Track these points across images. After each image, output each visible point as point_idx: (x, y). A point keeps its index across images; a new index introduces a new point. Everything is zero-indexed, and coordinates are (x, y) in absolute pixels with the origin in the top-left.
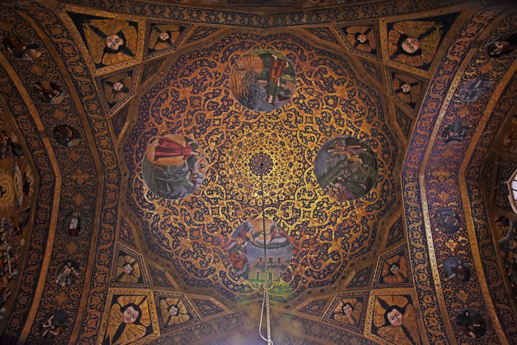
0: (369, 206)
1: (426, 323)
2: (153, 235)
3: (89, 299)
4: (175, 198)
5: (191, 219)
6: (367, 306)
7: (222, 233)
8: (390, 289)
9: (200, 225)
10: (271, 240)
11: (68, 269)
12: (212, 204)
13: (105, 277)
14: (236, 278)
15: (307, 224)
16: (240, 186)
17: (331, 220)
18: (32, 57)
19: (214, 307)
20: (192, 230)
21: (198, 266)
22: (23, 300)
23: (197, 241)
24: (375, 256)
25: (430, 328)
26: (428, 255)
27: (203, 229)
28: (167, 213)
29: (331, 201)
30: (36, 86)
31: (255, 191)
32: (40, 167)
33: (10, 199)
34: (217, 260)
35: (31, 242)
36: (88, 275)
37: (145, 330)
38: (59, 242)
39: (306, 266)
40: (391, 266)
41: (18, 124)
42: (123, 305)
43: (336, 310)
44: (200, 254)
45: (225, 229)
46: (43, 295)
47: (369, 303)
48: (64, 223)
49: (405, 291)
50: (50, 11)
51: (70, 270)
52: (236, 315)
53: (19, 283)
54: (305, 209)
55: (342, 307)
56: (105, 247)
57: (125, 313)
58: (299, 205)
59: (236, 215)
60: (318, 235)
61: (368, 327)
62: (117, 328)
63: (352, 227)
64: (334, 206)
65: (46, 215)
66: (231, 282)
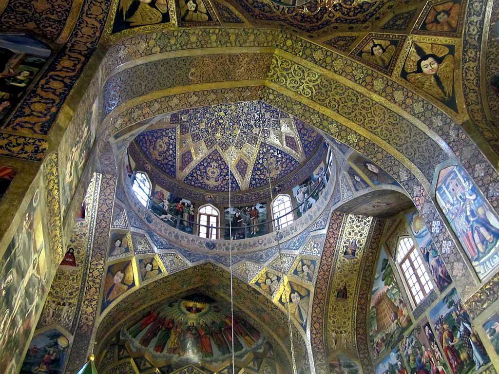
1: (464, 75)
8: (431, 37)
19: (233, 15)
25: (467, 80)
26: (485, 9)
37: (161, 16)
40: (439, 13)
47: (405, 46)
52: (255, 32)
55: (372, 48)
61: (397, 71)
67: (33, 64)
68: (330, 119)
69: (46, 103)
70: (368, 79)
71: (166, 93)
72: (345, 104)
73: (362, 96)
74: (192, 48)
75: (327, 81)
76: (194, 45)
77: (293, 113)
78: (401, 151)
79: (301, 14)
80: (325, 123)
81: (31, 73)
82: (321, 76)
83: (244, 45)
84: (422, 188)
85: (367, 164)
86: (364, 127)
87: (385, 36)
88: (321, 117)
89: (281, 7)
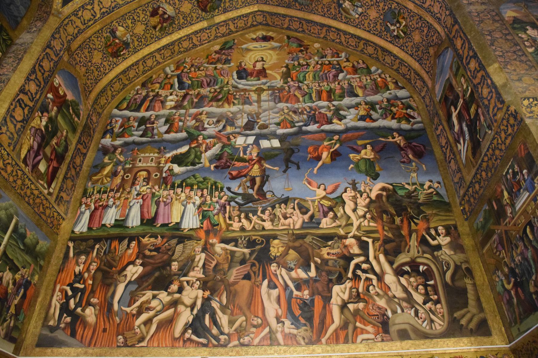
18: (126, 34)
22: (370, 50)
30: (157, 29)
32: (249, 25)
33: (270, 54)
35: (320, 38)
38: (320, 10)
41: (203, 44)
46: (368, 31)
48: (303, 4)
50: (63, 22)
51: (347, 2)
53: (355, 52)
65: (295, 21)
67: (458, 69)
69: (484, 84)
81: (463, 75)
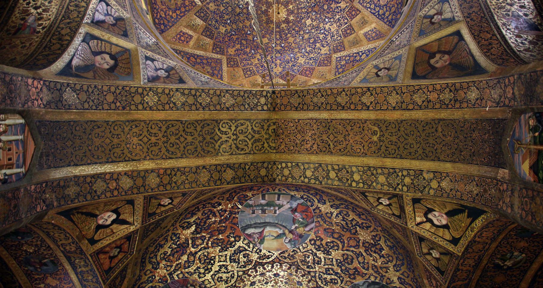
0: (151, 282)
1: (68, 235)
2: (402, 255)
3: (487, 247)
4: (374, 283)
5: (357, 258)
6: (143, 214)
7: (322, 240)
8: (118, 238)
9: (347, 250)
10: (263, 230)
11: (508, 264)
12: (332, 269)
13: (464, 262)
14: (305, 197)
15: (222, 249)
16: (300, 283)
17: (195, 257)
20: (357, 246)
21: (350, 213)
23: (351, 236)
24: (139, 251)
26: (78, 277)
27: (343, 246)
28: (384, 270)
29: (196, 276)
31: (283, 277)
34: (329, 215)
36: (485, 262)
37: (422, 202)
39: (221, 209)
40: (119, 253)
42: (446, 230)
43: (180, 198)
44: (349, 223)
45: (318, 243)
47: (140, 219)
49: (99, 245)
51: (506, 263)
52: (306, 180)
54: (224, 263)
55: (173, 201)
56: (460, 283)
57: (444, 222)
58: (232, 266)
59: (305, 255)
60: (209, 240)
61: (139, 201)
62: (456, 217)
63: (170, 255)
64: (192, 271)
66: (312, 194)
68: (187, 108)
70: (166, 179)
71: (407, 115)
72: (177, 137)
73: (164, 157)
74: (381, 168)
75: (209, 152)
76: (379, 171)
77: (231, 92)
78: (89, 124)
79: (254, 190)
80: (191, 100)
82: (217, 154)
83: (317, 165)
84: (42, 106)
85: (112, 62)
86: (144, 121)
87: (164, 214)
88: (198, 106)
89: (277, 191)
